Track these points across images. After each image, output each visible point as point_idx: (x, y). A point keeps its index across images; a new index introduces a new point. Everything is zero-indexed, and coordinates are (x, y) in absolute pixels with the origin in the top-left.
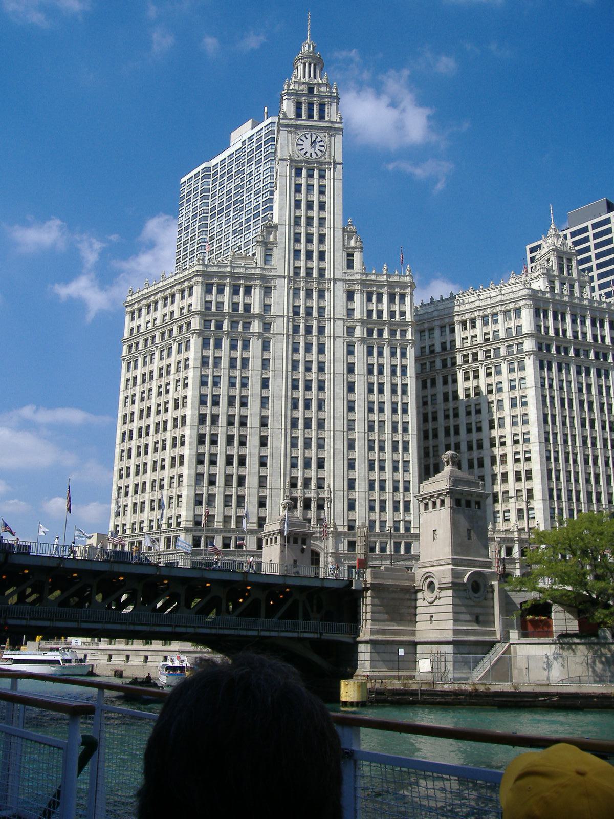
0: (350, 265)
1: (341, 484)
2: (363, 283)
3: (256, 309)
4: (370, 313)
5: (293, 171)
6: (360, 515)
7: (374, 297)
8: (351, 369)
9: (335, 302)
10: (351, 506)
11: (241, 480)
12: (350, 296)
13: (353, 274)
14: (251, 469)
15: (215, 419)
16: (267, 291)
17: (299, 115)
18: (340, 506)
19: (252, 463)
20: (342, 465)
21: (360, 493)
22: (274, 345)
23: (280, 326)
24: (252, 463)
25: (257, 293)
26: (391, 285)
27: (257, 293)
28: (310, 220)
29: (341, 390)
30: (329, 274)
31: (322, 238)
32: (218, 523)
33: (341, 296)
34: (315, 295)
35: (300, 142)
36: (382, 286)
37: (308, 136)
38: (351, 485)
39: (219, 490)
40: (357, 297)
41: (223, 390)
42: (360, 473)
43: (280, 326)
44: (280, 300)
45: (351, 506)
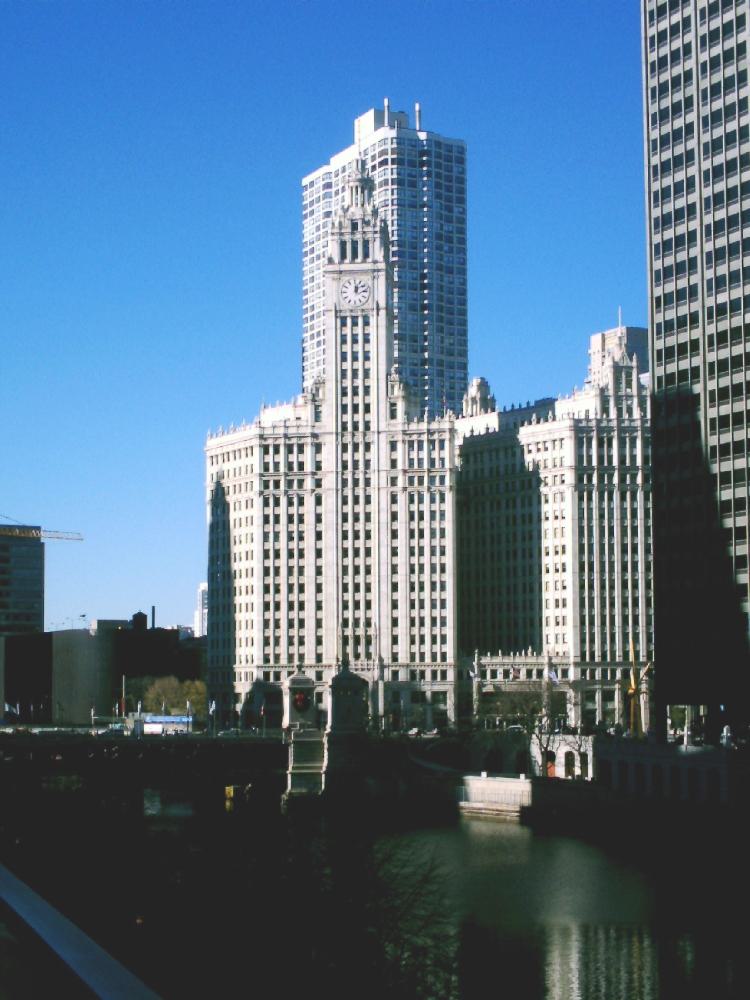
0: (393, 415)
1: (386, 623)
2: (404, 433)
3: (309, 467)
4: (411, 461)
5: (339, 320)
6: (402, 649)
7: (416, 445)
8: (394, 517)
9: (379, 455)
10: (395, 640)
11: (302, 623)
12: (393, 446)
13: (394, 425)
14: (309, 614)
15: (277, 571)
16: (318, 448)
17: (343, 256)
18: (386, 641)
19: (310, 607)
20: (386, 606)
21: (402, 630)
22: (326, 499)
23: (329, 482)
24: (310, 607)
25: (309, 450)
26: (430, 432)
27: (309, 450)
28: (355, 373)
29: (386, 536)
30: (373, 427)
31: (367, 390)
32: (284, 661)
33: (385, 447)
34: (361, 448)
35: (344, 289)
36: (420, 434)
37: (352, 282)
38: (395, 622)
39: (283, 632)
40: (400, 446)
41: (282, 545)
42: (402, 613)
43: (329, 482)
44: (329, 457)
45: (395, 640)
